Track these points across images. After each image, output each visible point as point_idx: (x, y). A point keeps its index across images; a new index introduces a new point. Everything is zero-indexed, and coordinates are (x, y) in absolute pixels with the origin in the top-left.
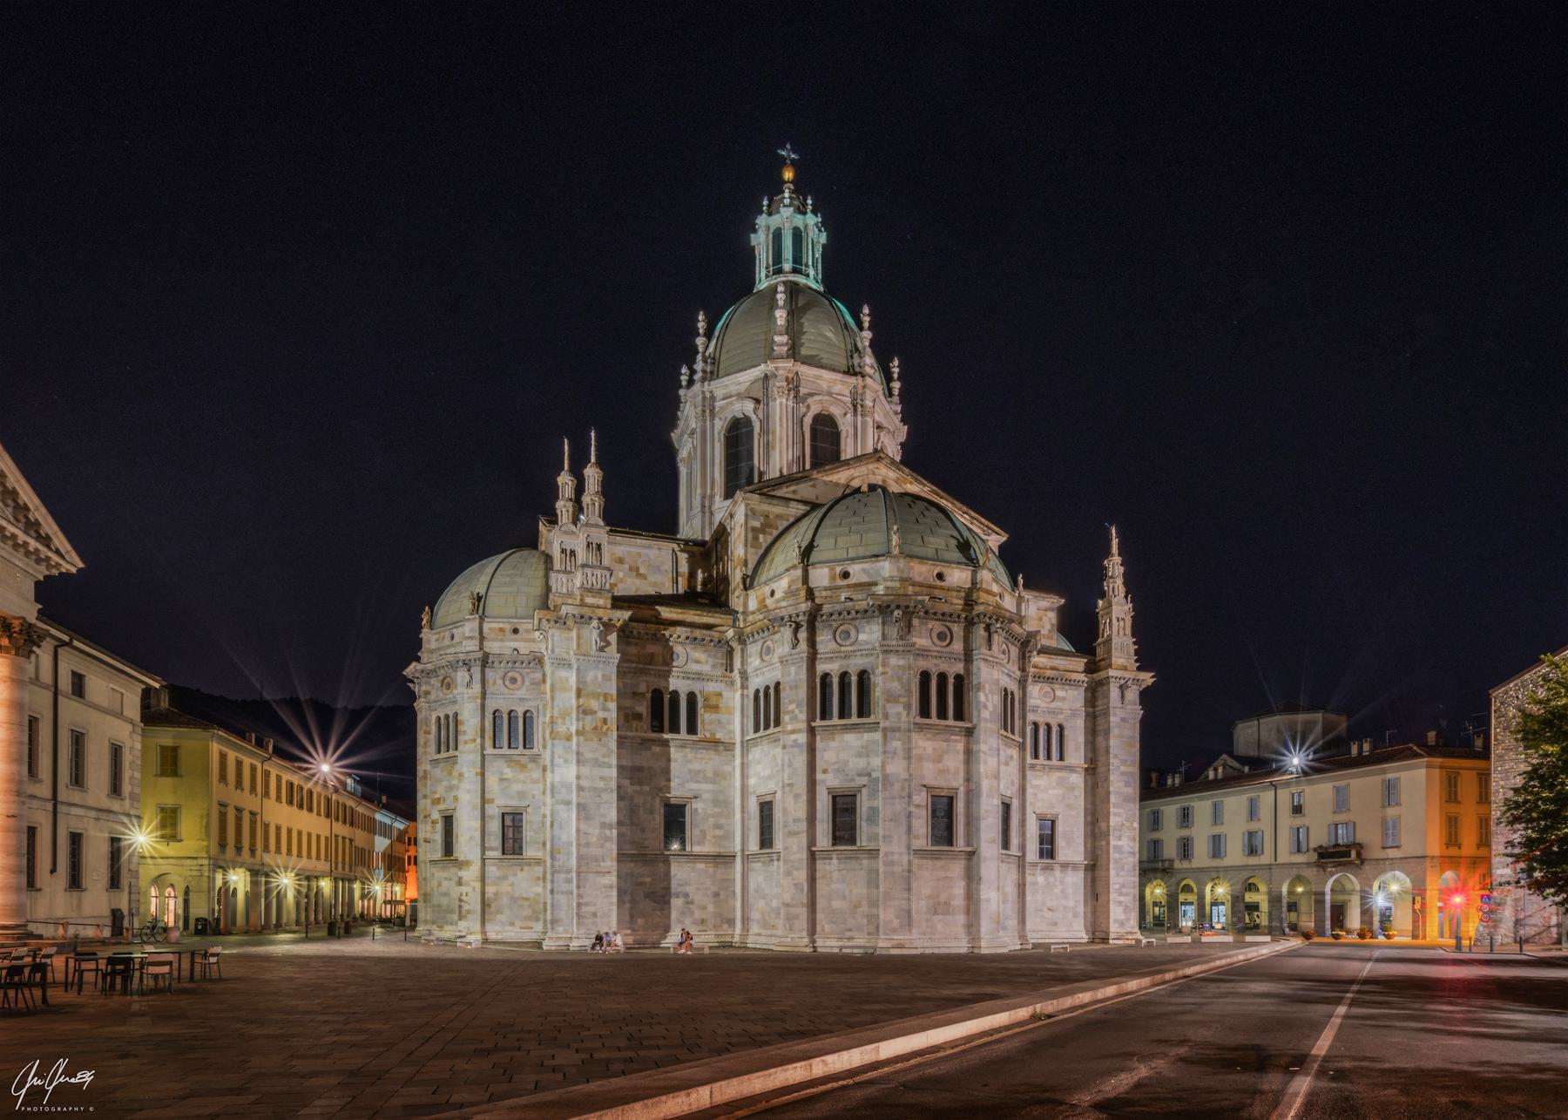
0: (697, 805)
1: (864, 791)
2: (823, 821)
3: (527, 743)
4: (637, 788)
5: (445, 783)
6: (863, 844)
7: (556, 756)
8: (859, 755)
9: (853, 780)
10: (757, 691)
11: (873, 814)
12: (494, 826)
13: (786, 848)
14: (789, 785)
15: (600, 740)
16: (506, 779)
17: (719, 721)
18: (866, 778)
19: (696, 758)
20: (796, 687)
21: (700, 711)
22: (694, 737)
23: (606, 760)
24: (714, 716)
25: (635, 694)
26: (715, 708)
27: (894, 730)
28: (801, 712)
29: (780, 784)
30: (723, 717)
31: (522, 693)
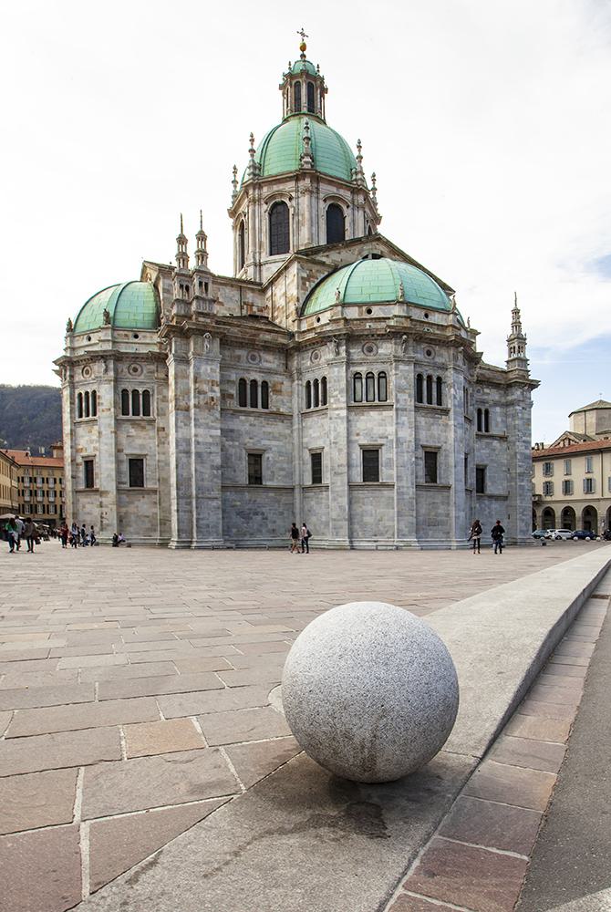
1: (383, 447)
3: (147, 413)
4: (231, 443)
5: (87, 438)
8: (380, 425)
9: (376, 441)
10: (309, 382)
12: (125, 467)
13: (333, 483)
17: (283, 402)
18: (385, 440)
20: (339, 381)
22: (266, 411)
24: (279, 397)
25: (229, 381)
26: (278, 392)
27: (405, 410)
29: (328, 443)
30: (286, 398)
31: (142, 378)
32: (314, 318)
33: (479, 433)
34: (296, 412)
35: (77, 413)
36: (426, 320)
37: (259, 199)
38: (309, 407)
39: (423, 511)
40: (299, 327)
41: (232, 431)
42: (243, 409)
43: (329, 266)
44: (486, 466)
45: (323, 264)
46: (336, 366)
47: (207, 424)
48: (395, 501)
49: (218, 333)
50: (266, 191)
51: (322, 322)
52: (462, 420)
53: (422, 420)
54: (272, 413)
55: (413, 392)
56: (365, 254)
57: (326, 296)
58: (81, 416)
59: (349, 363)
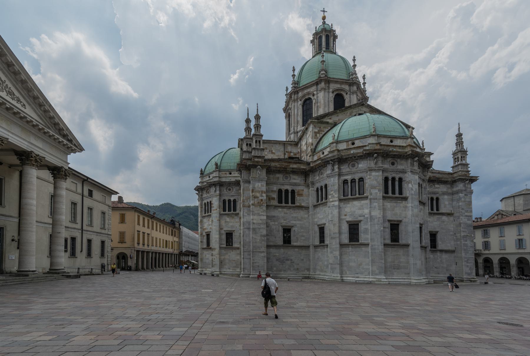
1: (362, 222)
2: (345, 233)
3: (235, 210)
4: (273, 223)
6: (362, 242)
7: (245, 213)
8: (360, 209)
11: (366, 231)
14: (331, 220)
15: (260, 207)
16: (227, 222)
18: (363, 217)
20: (334, 185)
22: (294, 205)
23: (262, 213)
27: (374, 199)
28: (335, 194)
29: (328, 221)
32: (321, 153)
33: (432, 212)
34: (311, 205)
35: (204, 212)
37: (297, 99)
38: (318, 201)
39: (389, 260)
40: (313, 159)
41: (274, 217)
43: (331, 124)
44: (437, 232)
46: (333, 177)
47: (259, 213)
48: (370, 254)
49: (265, 166)
51: (325, 154)
52: (417, 203)
53: (389, 205)
57: (328, 139)
59: (340, 175)
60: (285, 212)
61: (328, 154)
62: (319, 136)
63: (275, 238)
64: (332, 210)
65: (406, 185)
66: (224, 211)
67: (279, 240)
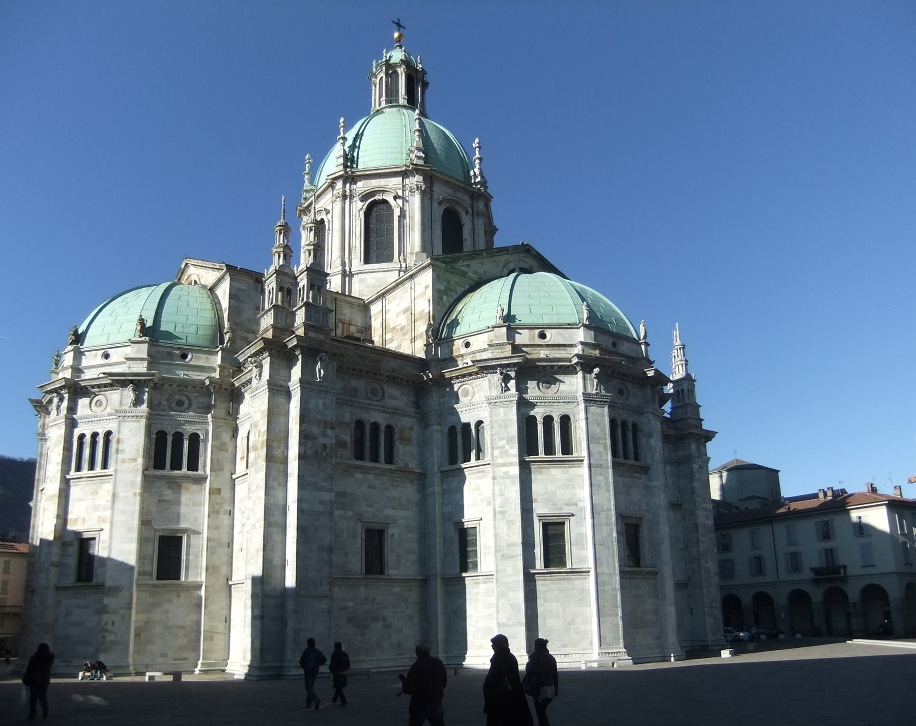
0: (392, 531)
3: (193, 465)
4: (341, 512)
7: (271, 479)
14: (500, 512)
15: (320, 465)
19: (392, 485)
20: (506, 426)
21: (397, 443)
23: (325, 484)
25: (341, 423)
27: (601, 466)
28: (511, 448)
36: (614, 349)
37: (352, 197)
42: (359, 463)
45: (465, 274)
50: (360, 184)
51: (473, 347)
54: (399, 470)
55: (609, 443)
56: (511, 266)
58: (78, 469)
60: (372, 483)
61: (485, 350)
62: (448, 301)
63: (346, 555)
64: (503, 488)
65: (644, 440)
66: (155, 468)
67: (356, 561)
